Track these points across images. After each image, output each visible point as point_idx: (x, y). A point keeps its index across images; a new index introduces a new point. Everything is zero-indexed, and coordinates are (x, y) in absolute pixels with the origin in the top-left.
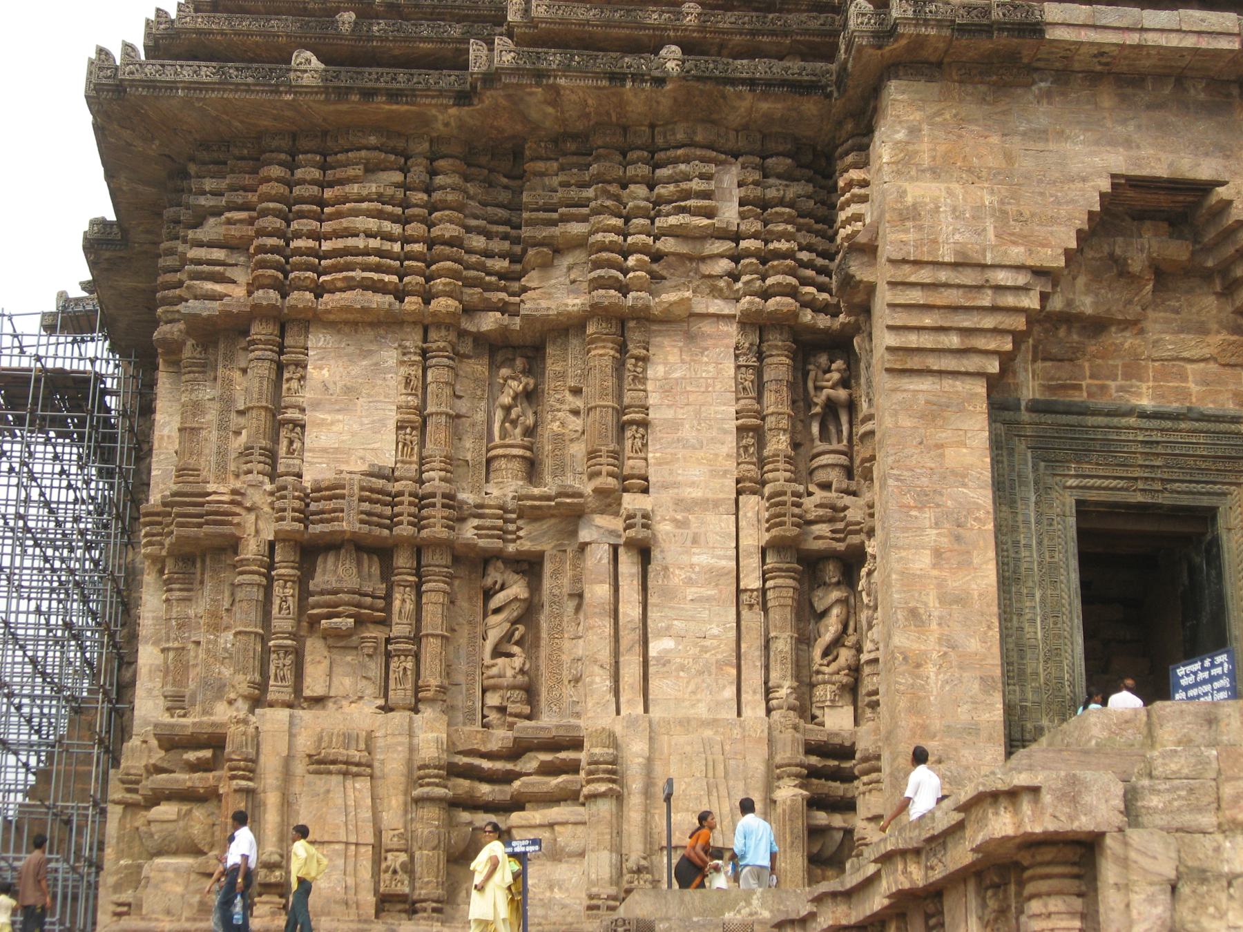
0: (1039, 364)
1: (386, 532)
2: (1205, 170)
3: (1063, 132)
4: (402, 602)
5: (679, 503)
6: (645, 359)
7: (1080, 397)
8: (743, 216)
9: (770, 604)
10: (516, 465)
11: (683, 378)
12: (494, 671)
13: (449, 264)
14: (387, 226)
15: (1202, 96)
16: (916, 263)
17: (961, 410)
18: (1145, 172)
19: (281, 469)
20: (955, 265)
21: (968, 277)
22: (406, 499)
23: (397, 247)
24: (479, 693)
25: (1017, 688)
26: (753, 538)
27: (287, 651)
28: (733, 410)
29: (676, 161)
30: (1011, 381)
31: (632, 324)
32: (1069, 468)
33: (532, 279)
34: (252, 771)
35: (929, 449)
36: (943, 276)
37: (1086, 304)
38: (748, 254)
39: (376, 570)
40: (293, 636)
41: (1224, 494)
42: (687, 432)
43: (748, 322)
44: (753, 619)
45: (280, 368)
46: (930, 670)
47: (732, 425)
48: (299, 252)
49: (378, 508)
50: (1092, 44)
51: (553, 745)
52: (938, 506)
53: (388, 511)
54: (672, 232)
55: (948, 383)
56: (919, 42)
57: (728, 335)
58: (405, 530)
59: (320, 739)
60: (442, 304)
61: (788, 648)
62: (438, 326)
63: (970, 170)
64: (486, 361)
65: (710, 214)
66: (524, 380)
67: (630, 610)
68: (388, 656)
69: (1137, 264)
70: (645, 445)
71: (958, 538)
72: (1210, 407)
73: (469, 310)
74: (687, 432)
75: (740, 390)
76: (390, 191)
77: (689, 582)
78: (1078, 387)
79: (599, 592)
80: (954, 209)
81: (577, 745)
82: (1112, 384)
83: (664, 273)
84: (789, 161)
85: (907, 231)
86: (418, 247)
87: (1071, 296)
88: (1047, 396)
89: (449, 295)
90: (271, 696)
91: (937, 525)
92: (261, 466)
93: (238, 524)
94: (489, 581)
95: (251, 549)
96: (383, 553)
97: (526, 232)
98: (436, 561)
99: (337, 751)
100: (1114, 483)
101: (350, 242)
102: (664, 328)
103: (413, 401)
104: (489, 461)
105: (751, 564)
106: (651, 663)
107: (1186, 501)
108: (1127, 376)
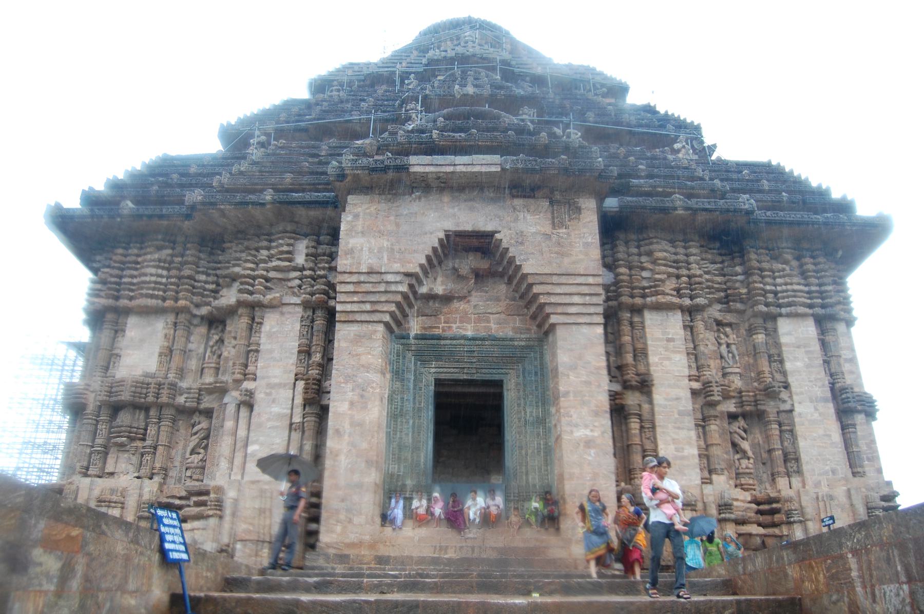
0: (420, 318)
1: (143, 400)
2: (487, 226)
3: (424, 213)
4: (152, 430)
5: (271, 386)
6: (261, 323)
7: (437, 332)
8: (306, 260)
9: (306, 429)
10: (212, 371)
11: (277, 331)
12: (189, 460)
13: (187, 287)
14: (160, 271)
15: (492, 195)
16: (350, 273)
17: (371, 338)
18: (461, 228)
19: (108, 375)
20: (368, 273)
21: (374, 278)
22: (153, 386)
23: (164, 280)
24: (184, 471)
25: (396, 466)
26: (299, 400)
27: (99, 452)
28: (297, 344)
29: (279, 238)
30: (407, 326)
31: (257, 309)
32: (432, 364)
33: (224, 292)
34: (220, 506)
35: (353, 356)
36: (362, 278)
37: (439, 289)
38: (307, 277)
39: (142, 416)
40: (105, 447)
41: (506, 374)
42: (276, 354)
43: (306, 305)
44: (296, 436)
45: (116, 332)
46: (342, 458)
47: (296, 350)
48: (125, 283)
49: (139, 390)
50: (432, 173)
51: (200, 493)
52: (354, 381)
53: (144, 391)
54: (276, 269)
55: (365, 326)
56: (356, 178)
57: (298, 312)
58: (151, 399)
59: (102, 492)
60: (181, 303)
61: (310, 449)
62: (182, 312)
63: (379, 232)
64: (206, 327)
65: (290, 260)
66: (220, 335)
67: (242, 433)
68: (142, 455)
69: (465, 269)
70: (256, 360)
71: (362, 396)
72: (501, 334)
73: (197, 306)
74: (276, 354)
75: (301, 335)
76: (163, 258)
77: (269, 420)
78: (439, 328)
79: (229, 424)
80: (370, 249)
81: (207, 493)
82: (454, 326)
83: (273, 287)
84: (329, 237)
85: (347, 259)
86: (173, 280)
87: (433, 286)
88: (423, 332)
89: (186, 299)
90: (89, 473)
91: (353, 390)
92: (100, 374)
93: (85, 398)
94: (192, 421)
95: (91, 408)
96: (146, 408)
97: (218, 272)
98: (168, 413)
99: (108, 497)
100: (453, 370)
101: (144, 278)
102: (271, 310)
103: (166, 344)
104: (203, 369)
105: (298, 411)
106: (248, 456)
107: (488, 377)
108: (461, 322)
